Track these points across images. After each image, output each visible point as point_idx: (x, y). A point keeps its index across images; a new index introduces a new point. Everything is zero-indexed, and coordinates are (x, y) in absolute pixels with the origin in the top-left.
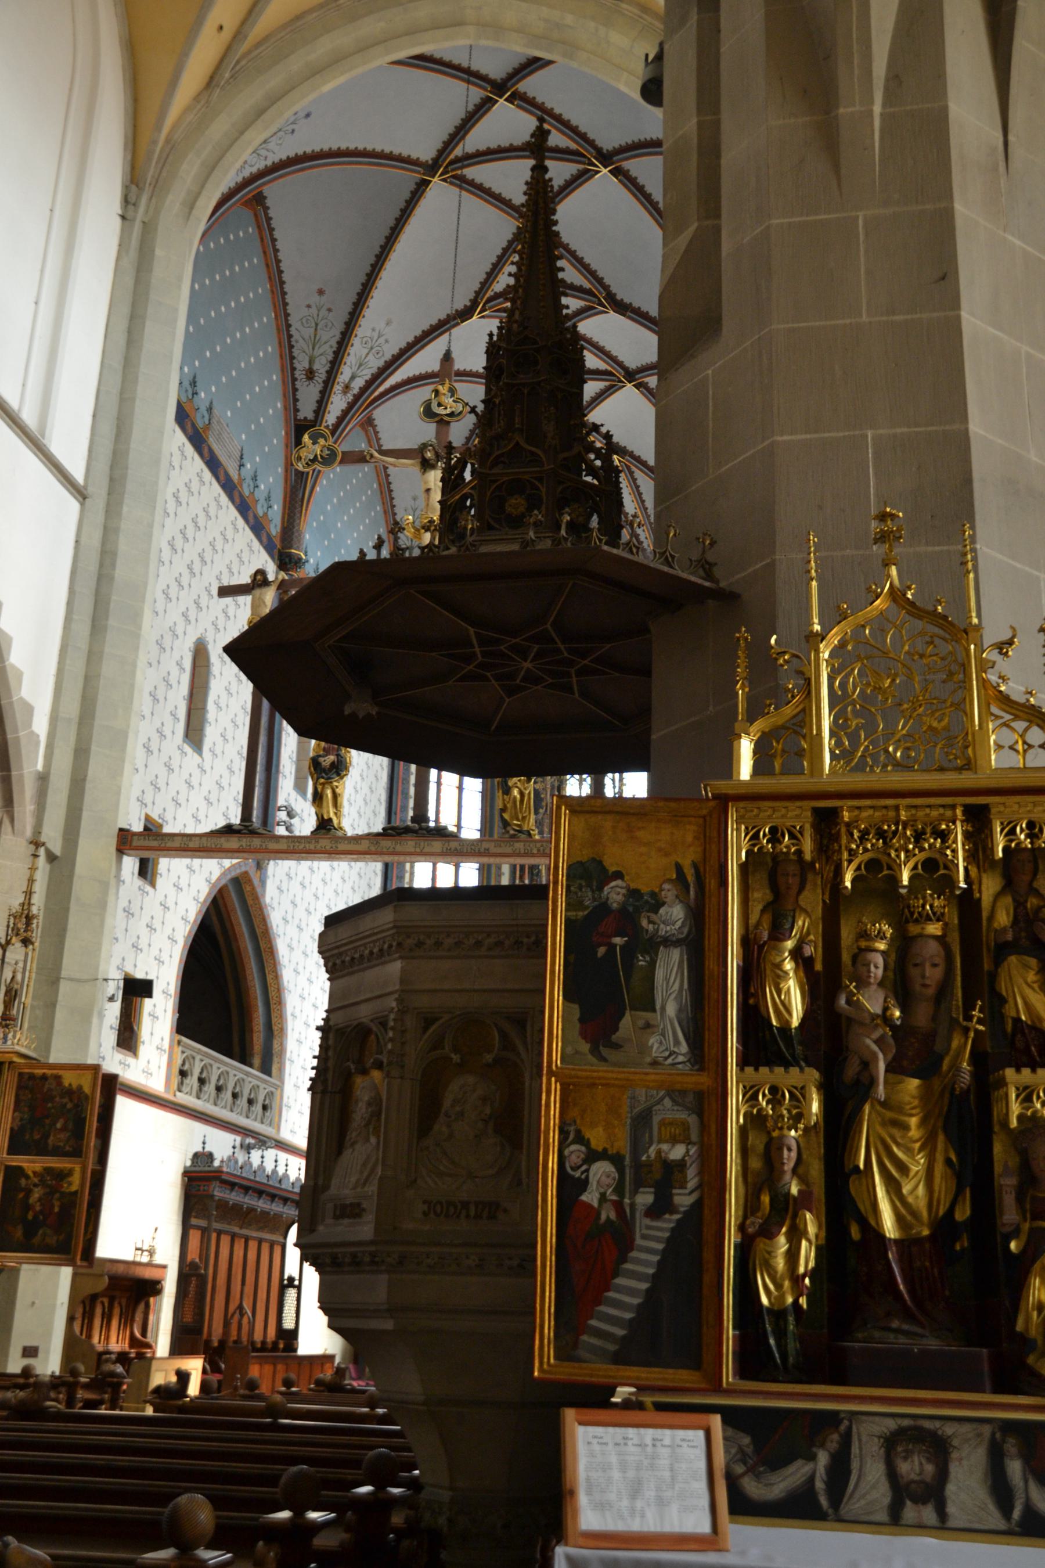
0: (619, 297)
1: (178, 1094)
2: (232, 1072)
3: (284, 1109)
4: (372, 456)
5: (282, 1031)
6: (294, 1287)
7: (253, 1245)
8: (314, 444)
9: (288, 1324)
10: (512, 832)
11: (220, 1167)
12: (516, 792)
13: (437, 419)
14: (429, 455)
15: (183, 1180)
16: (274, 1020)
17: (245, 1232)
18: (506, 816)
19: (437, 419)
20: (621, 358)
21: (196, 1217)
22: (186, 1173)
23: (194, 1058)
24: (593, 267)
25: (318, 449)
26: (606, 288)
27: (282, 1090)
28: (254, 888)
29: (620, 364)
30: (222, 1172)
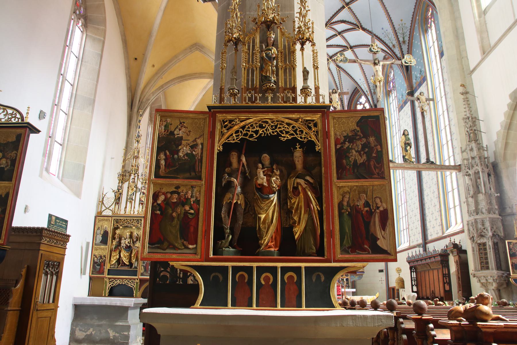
0: (363, 27)
4: (357, 61)
8: (341, 56)
10: (409, 162)
12: (409, 151)
13: (373, 52)
14: (377, 62)
18: (406, 157)
19: (373, 52)
20: (349, 43)
24: (358, 18)
25: (342, 58)
26: (360, 24)
29: (349, 44)
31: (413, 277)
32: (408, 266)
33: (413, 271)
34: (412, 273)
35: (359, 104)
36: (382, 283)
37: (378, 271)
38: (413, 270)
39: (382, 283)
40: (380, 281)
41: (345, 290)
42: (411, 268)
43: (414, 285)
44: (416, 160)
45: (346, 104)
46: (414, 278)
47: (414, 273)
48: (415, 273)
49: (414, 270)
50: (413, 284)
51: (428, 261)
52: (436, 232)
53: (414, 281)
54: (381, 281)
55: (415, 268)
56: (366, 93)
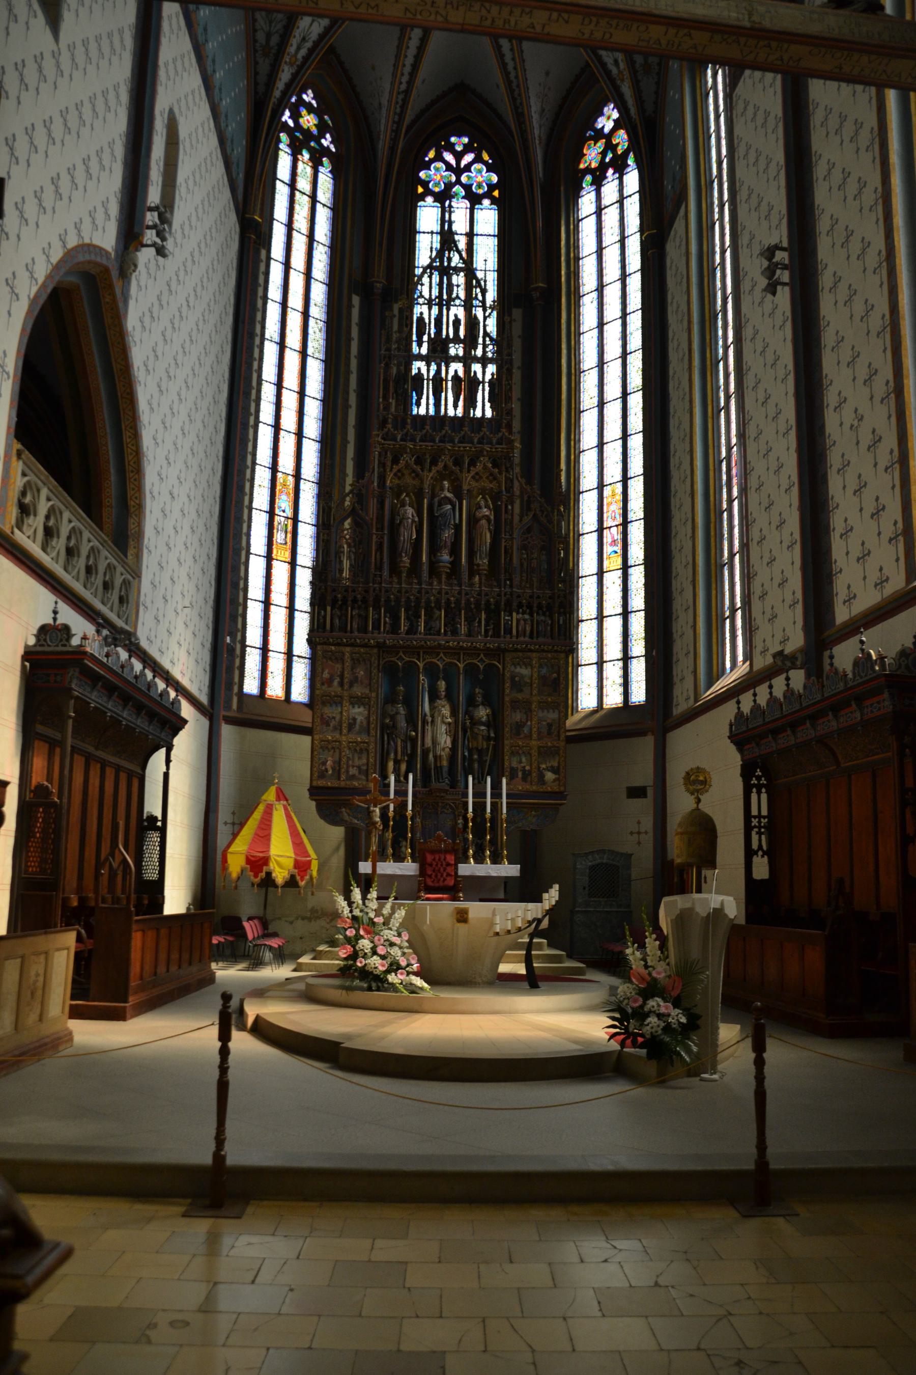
1: (16, 531)
2: (86, 535)
3: (141, 608)
5: (140, 507)
6: (157, 829)
7: (110, 773)
9: (151, 874)
11: (81, 646)
15: (23, 667)
16: (130, 493)
17: (100, 754)
21: (41, 724)
22: (29, 655)
23: (38, 491)
27: (140, 581)
28: (114, 300)
30: (85, 653)
31: (754, 812)
32: (734, 759)
33: (759, 788)
34: (754, 797)
35: (591, 138)
36: (639, 843)
37: (624, 794)
38: (759, 778)
39: (639, 843)
40: (632, 833)
41: (374, 867)
42: (747, 772)
43: (756, 853)
44: (790, 257)
45: (537, 132)
46: (759, 816)
47: (759, 793)
48: (764, 797)
49: (763, 781)
50: (755, 846)
51: (830, 724)
52: (874, 577)
53: (759, 834)
54: (636, 836)
55: (766, 774)
56: (614, 71)
